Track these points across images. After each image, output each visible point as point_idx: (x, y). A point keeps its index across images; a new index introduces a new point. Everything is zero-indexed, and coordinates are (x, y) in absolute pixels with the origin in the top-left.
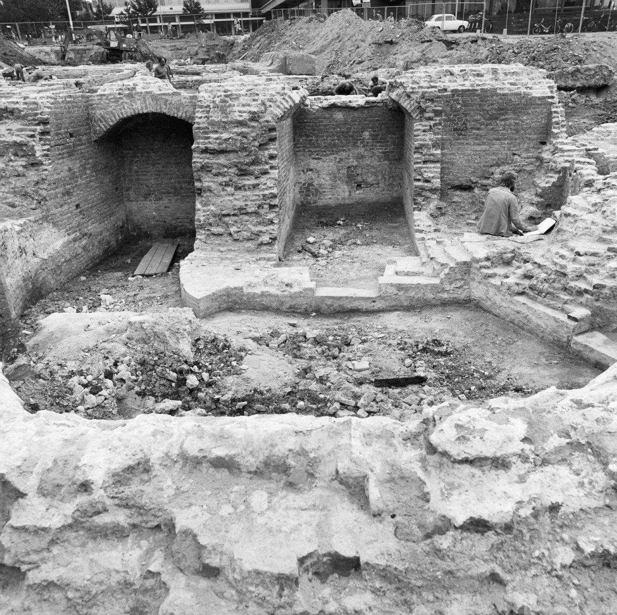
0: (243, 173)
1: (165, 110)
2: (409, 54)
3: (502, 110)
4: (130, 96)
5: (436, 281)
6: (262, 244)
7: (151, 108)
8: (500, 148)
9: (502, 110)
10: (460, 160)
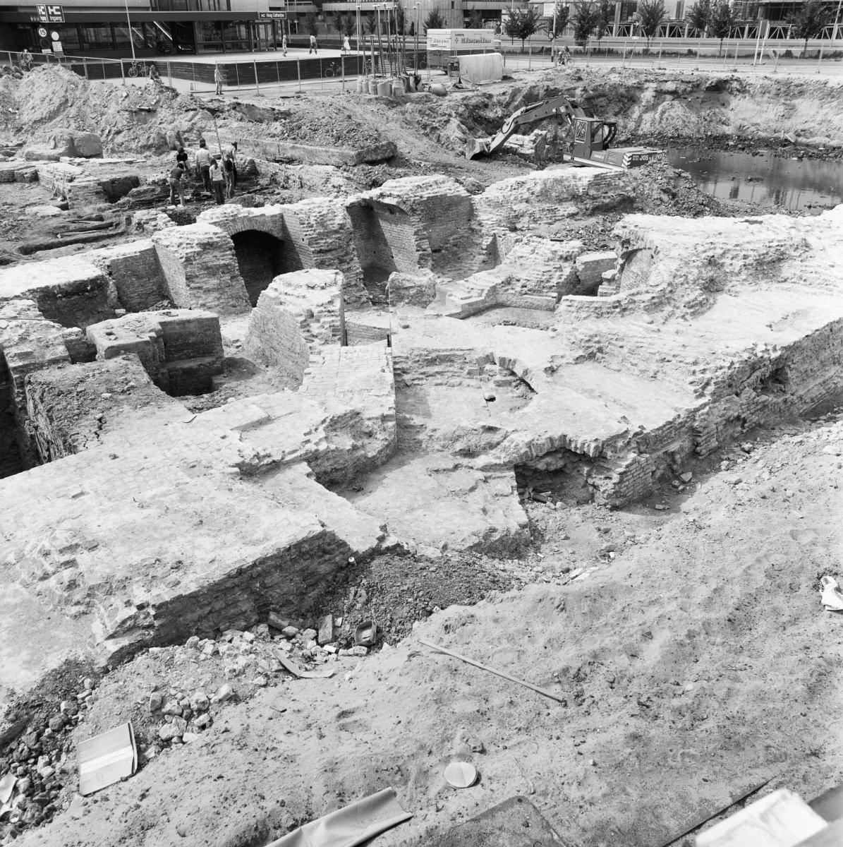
0: (341, 262)
2: (176, 123)
3: (450, 205)
4: (234, 221)
5: (482, 298)
7: (248, 228)
8: (451, 225)
9: (450, 205)
10: (434, 235)
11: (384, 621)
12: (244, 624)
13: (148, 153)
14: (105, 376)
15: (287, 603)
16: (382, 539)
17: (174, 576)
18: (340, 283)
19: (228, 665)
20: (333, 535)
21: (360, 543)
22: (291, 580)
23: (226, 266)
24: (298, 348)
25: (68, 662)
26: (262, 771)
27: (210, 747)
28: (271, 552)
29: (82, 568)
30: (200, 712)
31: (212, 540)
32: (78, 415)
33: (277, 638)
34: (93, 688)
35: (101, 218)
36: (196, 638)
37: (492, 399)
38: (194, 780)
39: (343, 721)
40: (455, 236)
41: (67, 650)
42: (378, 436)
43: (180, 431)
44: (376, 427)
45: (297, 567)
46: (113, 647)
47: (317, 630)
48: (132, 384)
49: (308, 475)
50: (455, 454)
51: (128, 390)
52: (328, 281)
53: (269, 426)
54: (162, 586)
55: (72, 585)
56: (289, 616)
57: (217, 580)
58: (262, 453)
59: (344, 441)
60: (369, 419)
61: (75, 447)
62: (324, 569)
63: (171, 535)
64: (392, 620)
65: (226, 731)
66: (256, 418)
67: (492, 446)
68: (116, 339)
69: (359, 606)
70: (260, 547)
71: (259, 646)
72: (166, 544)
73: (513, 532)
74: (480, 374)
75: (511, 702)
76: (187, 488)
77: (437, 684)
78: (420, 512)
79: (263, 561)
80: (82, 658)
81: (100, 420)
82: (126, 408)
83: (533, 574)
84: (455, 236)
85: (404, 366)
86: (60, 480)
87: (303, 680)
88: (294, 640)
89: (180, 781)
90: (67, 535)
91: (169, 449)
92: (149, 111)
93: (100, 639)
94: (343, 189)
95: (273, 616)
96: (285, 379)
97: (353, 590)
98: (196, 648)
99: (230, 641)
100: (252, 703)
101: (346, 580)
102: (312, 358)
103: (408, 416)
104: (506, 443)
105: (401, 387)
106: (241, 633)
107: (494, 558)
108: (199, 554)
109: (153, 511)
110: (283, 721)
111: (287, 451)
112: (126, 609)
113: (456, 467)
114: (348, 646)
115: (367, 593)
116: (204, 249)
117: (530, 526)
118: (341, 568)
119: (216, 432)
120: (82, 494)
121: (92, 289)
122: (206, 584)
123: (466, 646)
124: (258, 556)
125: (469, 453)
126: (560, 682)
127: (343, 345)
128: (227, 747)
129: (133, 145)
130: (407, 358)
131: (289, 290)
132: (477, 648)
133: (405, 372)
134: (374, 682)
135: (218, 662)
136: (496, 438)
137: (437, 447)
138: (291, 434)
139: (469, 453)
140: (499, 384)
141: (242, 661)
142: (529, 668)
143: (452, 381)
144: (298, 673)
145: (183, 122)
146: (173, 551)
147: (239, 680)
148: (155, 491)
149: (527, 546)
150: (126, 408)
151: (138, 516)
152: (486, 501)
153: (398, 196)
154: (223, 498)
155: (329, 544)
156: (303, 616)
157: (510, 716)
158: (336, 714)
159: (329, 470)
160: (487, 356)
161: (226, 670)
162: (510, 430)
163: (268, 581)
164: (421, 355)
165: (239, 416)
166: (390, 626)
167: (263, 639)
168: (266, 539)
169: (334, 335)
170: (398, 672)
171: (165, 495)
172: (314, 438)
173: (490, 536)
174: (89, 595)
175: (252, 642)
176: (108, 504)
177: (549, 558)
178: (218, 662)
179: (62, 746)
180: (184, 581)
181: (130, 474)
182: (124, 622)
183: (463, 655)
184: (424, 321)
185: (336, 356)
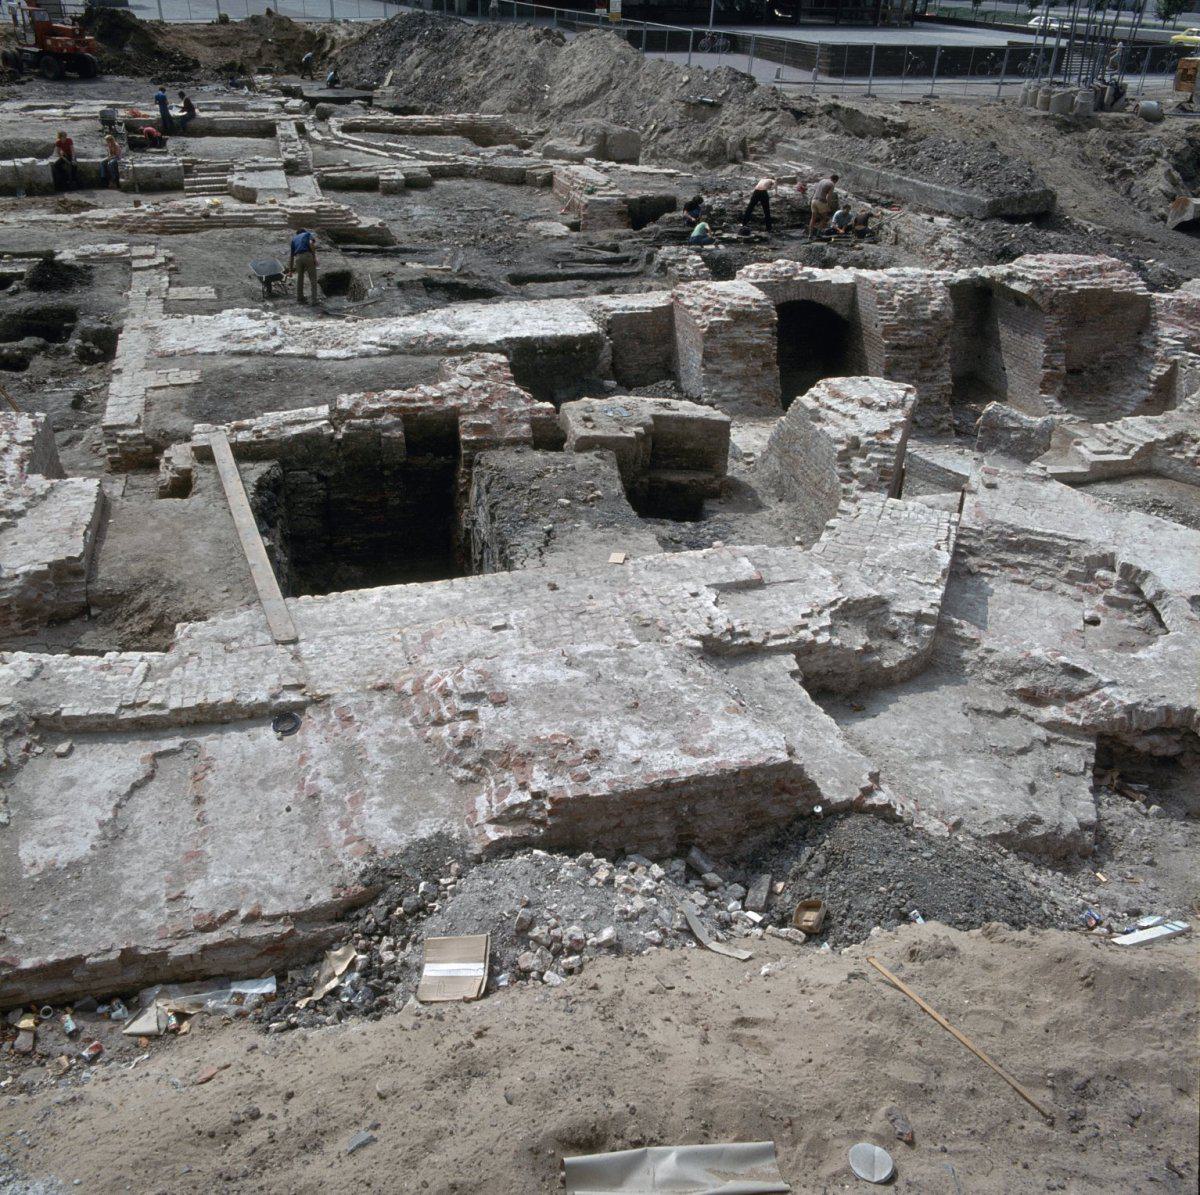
0: (924, 366)
1: (814, 298)
2: (745, 125)
6: (943, 430)
11: (837, 907)
12: (655, 852)
13: (697, 163)
14: (568, 475)
15: (717, 841)
16: (868, 792)
17: (585, 768)
18: (909, 405)
19: (619, 903)
20: (800, 769)
21: (833, 790)
22: (731, 814)
23: (759, 346)
24: (827, 486)
25: (439, 835)
26: (620, 1059)
27: (570, 1003)
28: (712, 771)
29: (482, 725)
30: (572, 951)
31: (644, 733)
32: (524, 520)
33: (693, 883)
34: (460, 877)
35: (615, 249)
36: (591, 856)
37: (1094, 622)
38: (539, 1040)
39: (738, 1030)
40: (1109, 354)
41: (442, 820)
42: (905, 641)
43: (643, 572)
44: (905, 627)
45: (742, 800)
46: (493, 834)
47: (747, 888)
48: (599, 492)
49: (793, 674)
50: (1012, 693)
51: (592, 500)
52: (893, 398)
53: (759, 593)
54: (568, 776)
55: (466, 742)
56: (716, 858)
57: (635, 788)
58: (739, 629)
59: (858, 640)
60: (899, 614)
61: (512, 562)
62: (776, 811)
63: (595, 712)
64: (849, 909)
65: (595, 988)
66: (743, 577)
67: (1071, 696)
68: (594, 427)
69: (810, 875)
70: (702, 761)
71: (666, 889)
72: (586, 723)
73: (1067, 830)
74: (1086, 581)
75: (973, 1091)
76: (632, 653)
77: (875, 1028)
78: (936, 764)
79: (698, 780)
80: (455, 836)
81: (549, 532)
82: (584, 525)
83: (1080, 901)
84: (1109, 354)
85: (973, 543)
86: (485, 602)
87: (707, 953)
88: (713, 893)
89: (523, 1034)
90: (475, 678)
91: (622, 594)
92: (712, 105)
93: (481, 819)
94: (955, 255)
95: (694, 854)
96: (800, 524)
97: (808, 850)
98: (588, 868)
99: (633, 871)
100: (636, 962)
101: (803, 834)
102: (843, 505)
103: (956, 621)
104: (1093, 697)
105: (960, 574)
106: (648, 863)
107: (1027, 861)
108: (623, 748)
109: (580, 674)
110: (665, 1001)
111: (774, 632)
112: (519, 793)
113: (1008, 712)
114: (782, 923)
115: (827, 861)
116: (736, 320)
117: (1097, 828)
118: (801, 817)
119: (685, 585)
120: (504, 627)
121: (582, 349)
122: (621, 790)
123: (932, 989)
124: (695, 772)
125: (1033, 697)
126: (1052, 1087)
127: (891, 495)
128: (589, 1010)
129: (681, 150)
130: (980, 533)
131: (834, 403)
132: (946, 996)
133: (972, 552)
134: (795, 992)
135: (609, 894)
136: (1082, 686)
137: (987, 675)
138: (784, 610)
139: (1033, 697)
140: (1111, 602)
141: (639, 903)
142: (1014, 1051)
143: (1041, 581)
144: (705, 939)
145: (754, 126)
146: (595, 732)
147: (629, 927)
148: (591, 648)
149: (1085, 857)
150: (584, 525)
151: (562, 675)
152: (1039, 772)
153: (1034, 281)
154: (672, 681)
155: (792, 781)
156: (735, 864)
157: (965, 1108)
158: (734, 1018)
159: (824, 671)
160: (1105, 556)
161: (616, 909)
162: (1106, 680)
163: (699, 807)
164: (1002, 533)
165: (722, 569)
166: (844, 916)
167: (675, 880)
168: (711, 751)
169: (881, 480)
170: (829, 990)
171: (601, 655)
172: (814, 624)
173: (1030, 828)
174: (481, 761)
175: (658, 880)
176: (531, 649)
177: (1108, 882)
178: (609, 894)
179: (410, 933)
180: (596, 778)
181: (567, 615)
182: (513, 807)
183: (925, 1000)
184: (1019, 483)
185: (876, 510)
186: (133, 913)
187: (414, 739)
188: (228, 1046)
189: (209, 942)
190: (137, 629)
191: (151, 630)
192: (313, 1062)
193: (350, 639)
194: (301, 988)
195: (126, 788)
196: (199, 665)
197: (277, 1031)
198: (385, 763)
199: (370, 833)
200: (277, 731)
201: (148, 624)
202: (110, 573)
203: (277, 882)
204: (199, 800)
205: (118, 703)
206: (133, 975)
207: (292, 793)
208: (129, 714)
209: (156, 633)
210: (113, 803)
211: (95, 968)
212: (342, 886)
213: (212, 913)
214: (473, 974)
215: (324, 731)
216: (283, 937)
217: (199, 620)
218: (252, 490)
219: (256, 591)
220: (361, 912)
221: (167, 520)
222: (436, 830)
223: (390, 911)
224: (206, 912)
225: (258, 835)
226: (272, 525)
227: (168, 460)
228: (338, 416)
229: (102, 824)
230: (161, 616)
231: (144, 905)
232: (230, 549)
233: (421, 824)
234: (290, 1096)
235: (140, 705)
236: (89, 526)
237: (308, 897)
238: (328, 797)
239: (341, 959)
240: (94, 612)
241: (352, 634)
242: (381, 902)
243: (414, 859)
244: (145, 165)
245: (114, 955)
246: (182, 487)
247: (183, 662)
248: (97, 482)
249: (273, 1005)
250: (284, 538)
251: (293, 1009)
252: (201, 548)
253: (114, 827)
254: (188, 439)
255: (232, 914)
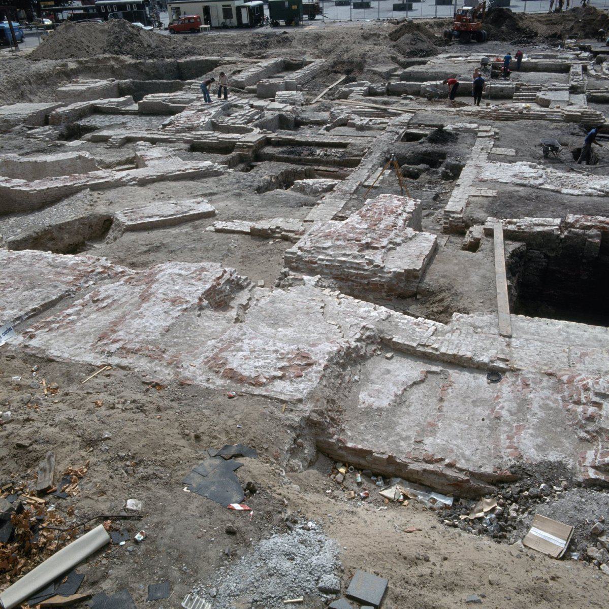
25: (560, 463)
34: (565, 489)
41: (564, 456)
179: (529, 507)
186: (398, 441)
187: (560, 407)
188: (423, 521)
189: (428, 468)
190: (435, 310)
191: (441, 312)
192: (461, 548)
193: (539, 344)
194: (464, 509)
195: (410, 383)
196: (459, 335)
197: (447, 524)
198: (541, 414)
199: (521, 447)
200: (488, 378)
201: (441, 309)
202: (430, 281)
203: (467, 453)
204: (441, 400)
205: (418, 342)
206: (391, 469)
207: (487, 412)
208: (421, 349)
209: (443, 314)
210: (403, 388)
211: (376, 459)
212: (500, 468)
213: (433, 455)
214: (558, 544)
215: (512, 387)
216: (463, 481)
217: (465, 313)
218: (508, 255)
219: (496, 306)
220: (506, 485)
221: (463, 261)
222: (559, 459)
223: (521, 491)
224: (430, 454)
225: (465, 426)
226: (514, 275)
227: (471, 232)
228: (565, 225)
229: (396, 395)
230: (448, 307)
231: (404, 439)
232: (489, 282)
233: (551, 453)
234: (446, 559)
235: (427, 346)
236: (426, 256)
237: (481, 467)
238: (505, 421)
239: (489, 504)
240: (418, 297)
241: (541, 341)
242: (517, 484)
243: (542, 470)
244: (497, 85)
245: (385, 457)
246: (474, 246)
247: (452, 331)
248: (436, 236)
249: (449, 512)
250: (518, 282)
251: (457, 518)
252: (475, 278)
253: (401, 399)
254: (483, 223)
255: (442, 460)
